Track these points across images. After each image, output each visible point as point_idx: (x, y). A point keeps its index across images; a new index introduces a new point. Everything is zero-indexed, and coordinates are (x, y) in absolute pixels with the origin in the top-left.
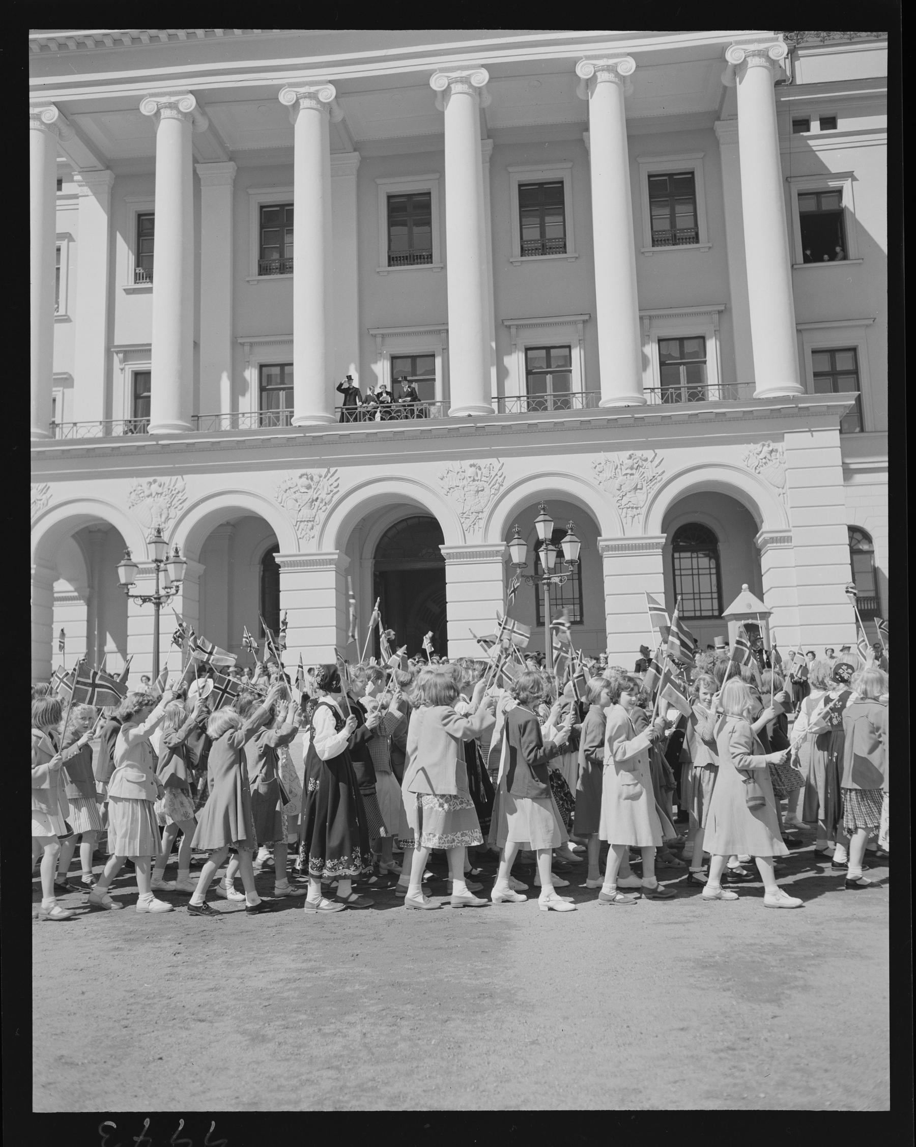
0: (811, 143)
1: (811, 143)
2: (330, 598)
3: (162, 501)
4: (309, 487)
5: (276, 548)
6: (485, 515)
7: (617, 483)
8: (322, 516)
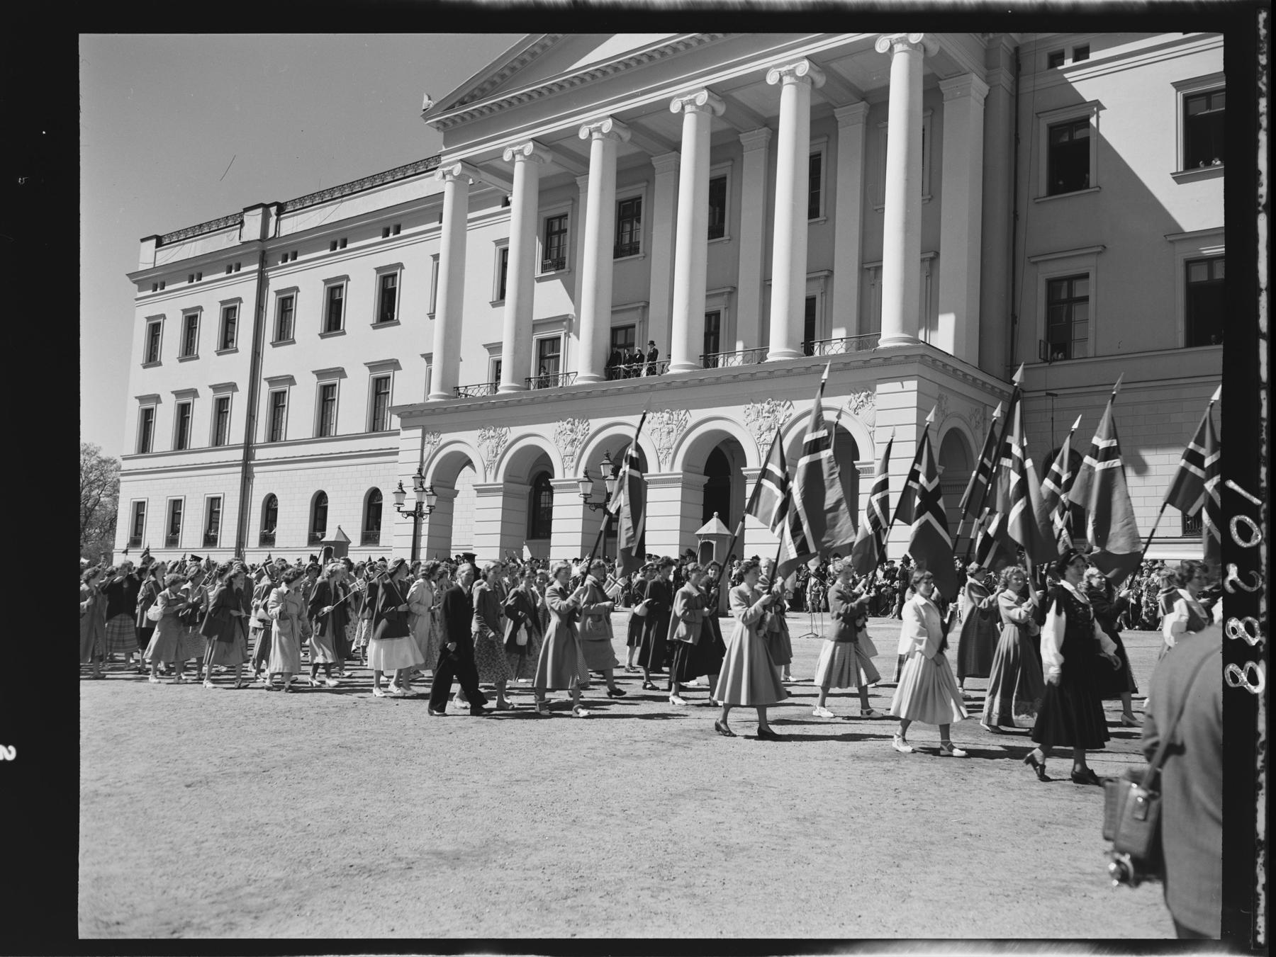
0: (1066, 76)
1: (1066, 76)
2: (676, 508)
3: (494, 441)
4: (572, 431)
5: (549, 473)
6: (672, 451)
7: (758, 424)
8: (578, 451)
